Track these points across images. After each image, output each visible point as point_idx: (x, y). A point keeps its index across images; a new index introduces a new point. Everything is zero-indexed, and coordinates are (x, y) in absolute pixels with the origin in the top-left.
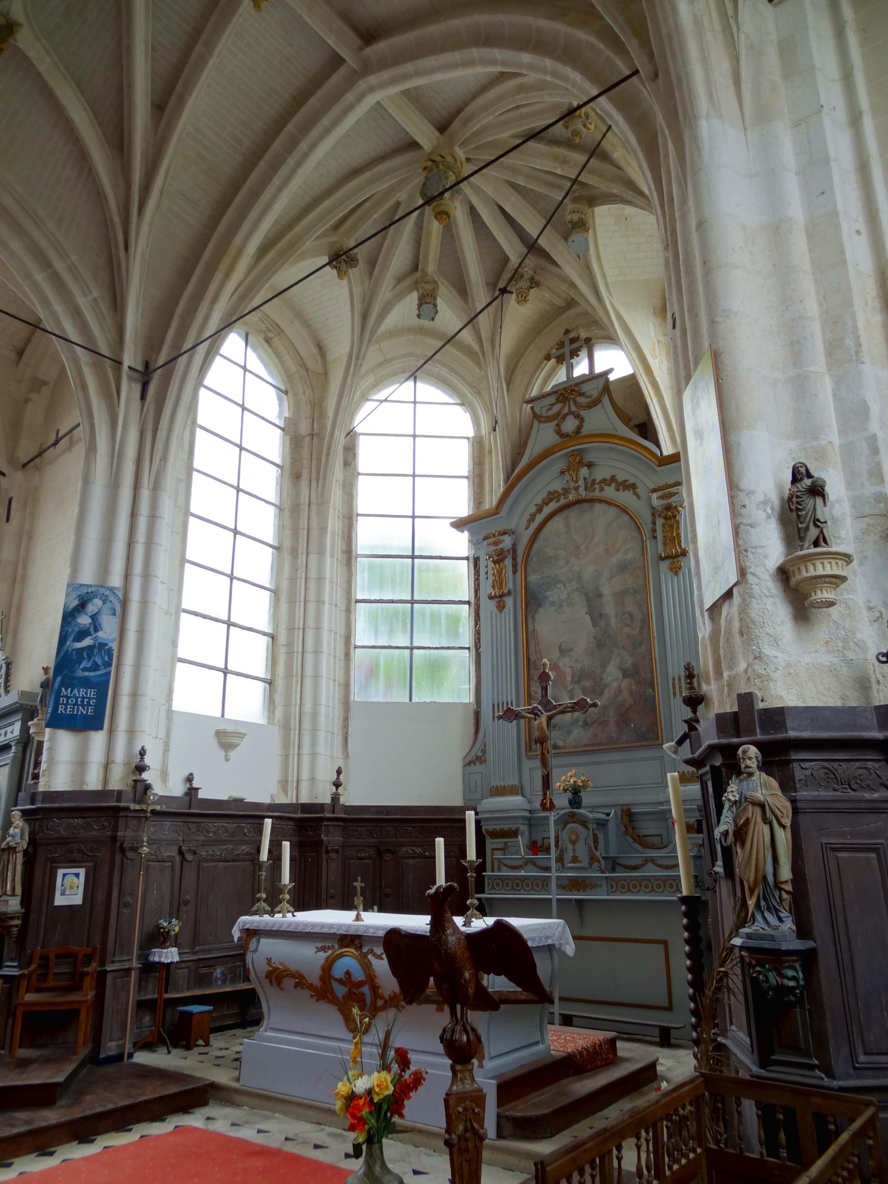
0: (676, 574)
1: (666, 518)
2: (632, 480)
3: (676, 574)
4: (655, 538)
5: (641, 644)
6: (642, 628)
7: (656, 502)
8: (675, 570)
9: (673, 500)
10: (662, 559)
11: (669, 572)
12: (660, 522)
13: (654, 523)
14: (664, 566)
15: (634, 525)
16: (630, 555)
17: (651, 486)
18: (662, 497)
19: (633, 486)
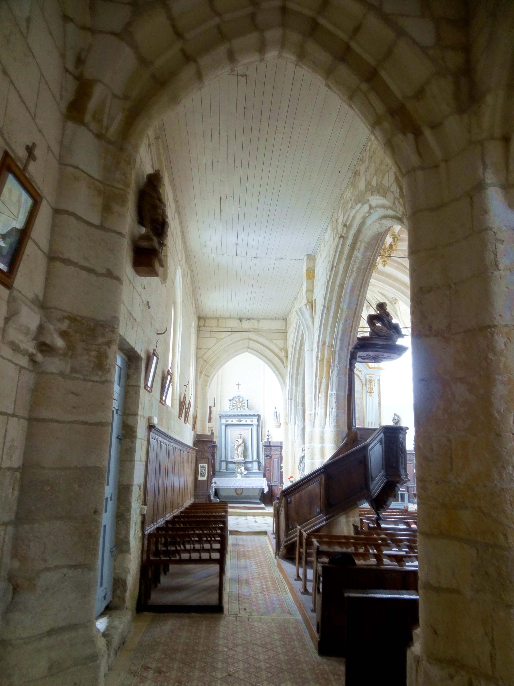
0: (371, 397)
1: (370, 382)
2: (360, 369)
3: (371, 397)
4: (366, 386)
5: (360, 412)
6: (361, 408)
7: (368, 377)
8: (371, 396)
9: (372, 378)
10: (368, 392)
11: (369, 396)
12: (368, 383)
13: (366, 383)
14: (368, 394)
15: (360, 381)
16: (359, 389)
17: (366, 373)
18: (370, 377)
19: (360, 371)
